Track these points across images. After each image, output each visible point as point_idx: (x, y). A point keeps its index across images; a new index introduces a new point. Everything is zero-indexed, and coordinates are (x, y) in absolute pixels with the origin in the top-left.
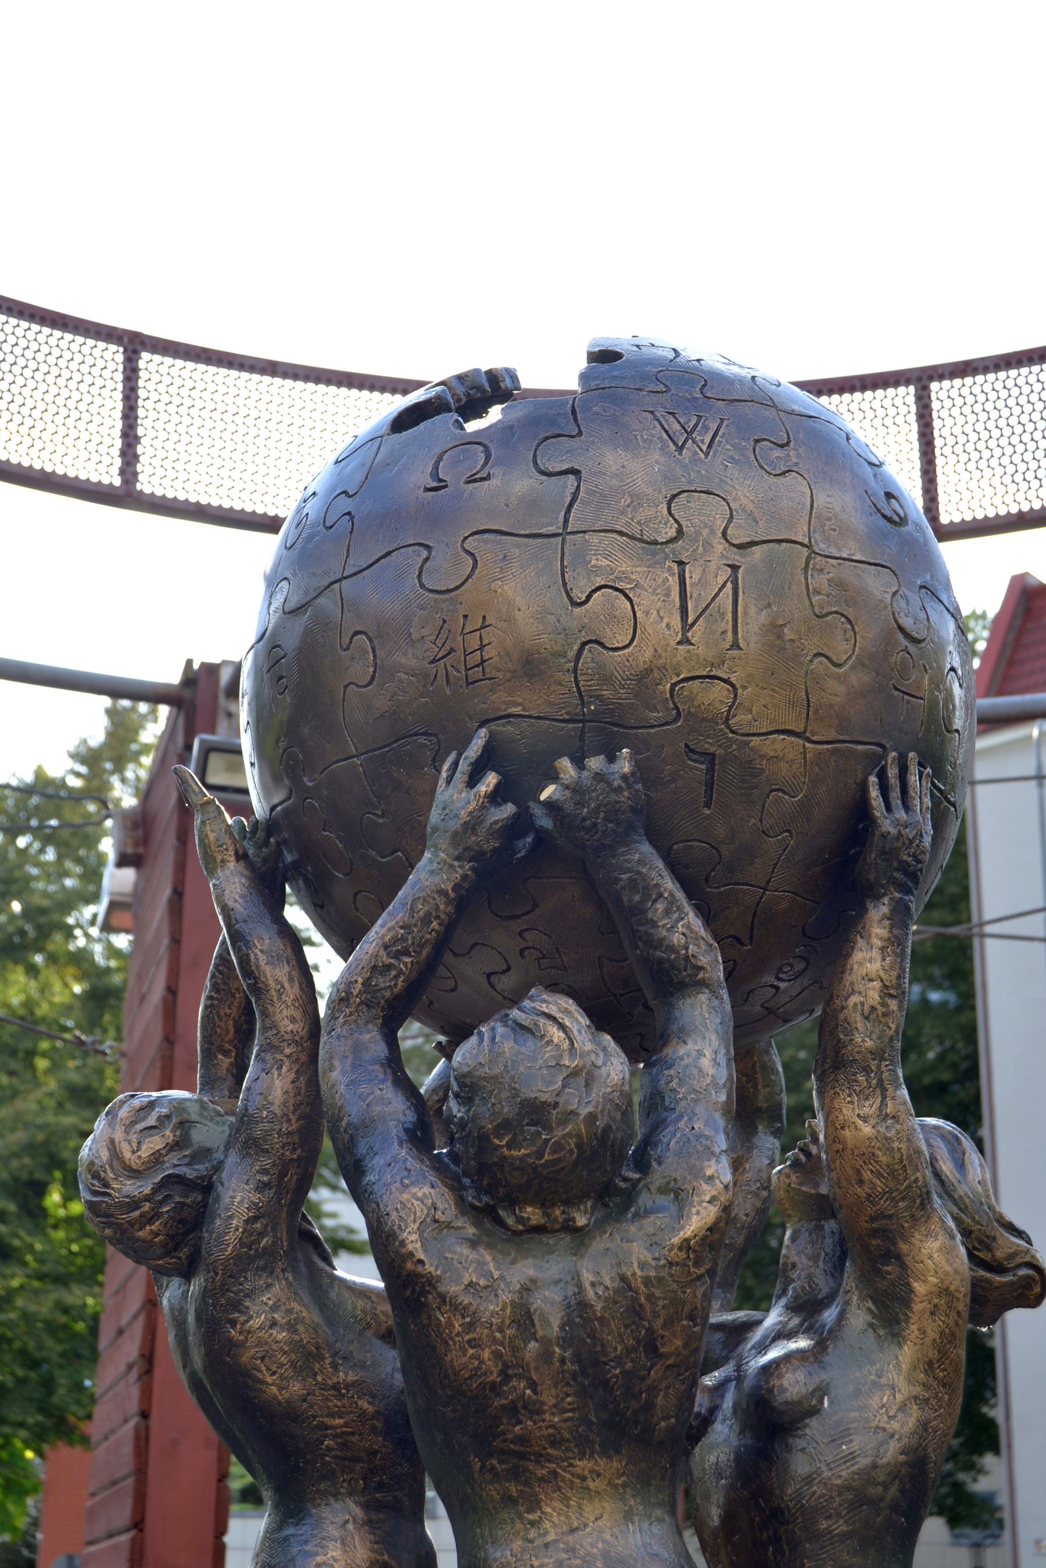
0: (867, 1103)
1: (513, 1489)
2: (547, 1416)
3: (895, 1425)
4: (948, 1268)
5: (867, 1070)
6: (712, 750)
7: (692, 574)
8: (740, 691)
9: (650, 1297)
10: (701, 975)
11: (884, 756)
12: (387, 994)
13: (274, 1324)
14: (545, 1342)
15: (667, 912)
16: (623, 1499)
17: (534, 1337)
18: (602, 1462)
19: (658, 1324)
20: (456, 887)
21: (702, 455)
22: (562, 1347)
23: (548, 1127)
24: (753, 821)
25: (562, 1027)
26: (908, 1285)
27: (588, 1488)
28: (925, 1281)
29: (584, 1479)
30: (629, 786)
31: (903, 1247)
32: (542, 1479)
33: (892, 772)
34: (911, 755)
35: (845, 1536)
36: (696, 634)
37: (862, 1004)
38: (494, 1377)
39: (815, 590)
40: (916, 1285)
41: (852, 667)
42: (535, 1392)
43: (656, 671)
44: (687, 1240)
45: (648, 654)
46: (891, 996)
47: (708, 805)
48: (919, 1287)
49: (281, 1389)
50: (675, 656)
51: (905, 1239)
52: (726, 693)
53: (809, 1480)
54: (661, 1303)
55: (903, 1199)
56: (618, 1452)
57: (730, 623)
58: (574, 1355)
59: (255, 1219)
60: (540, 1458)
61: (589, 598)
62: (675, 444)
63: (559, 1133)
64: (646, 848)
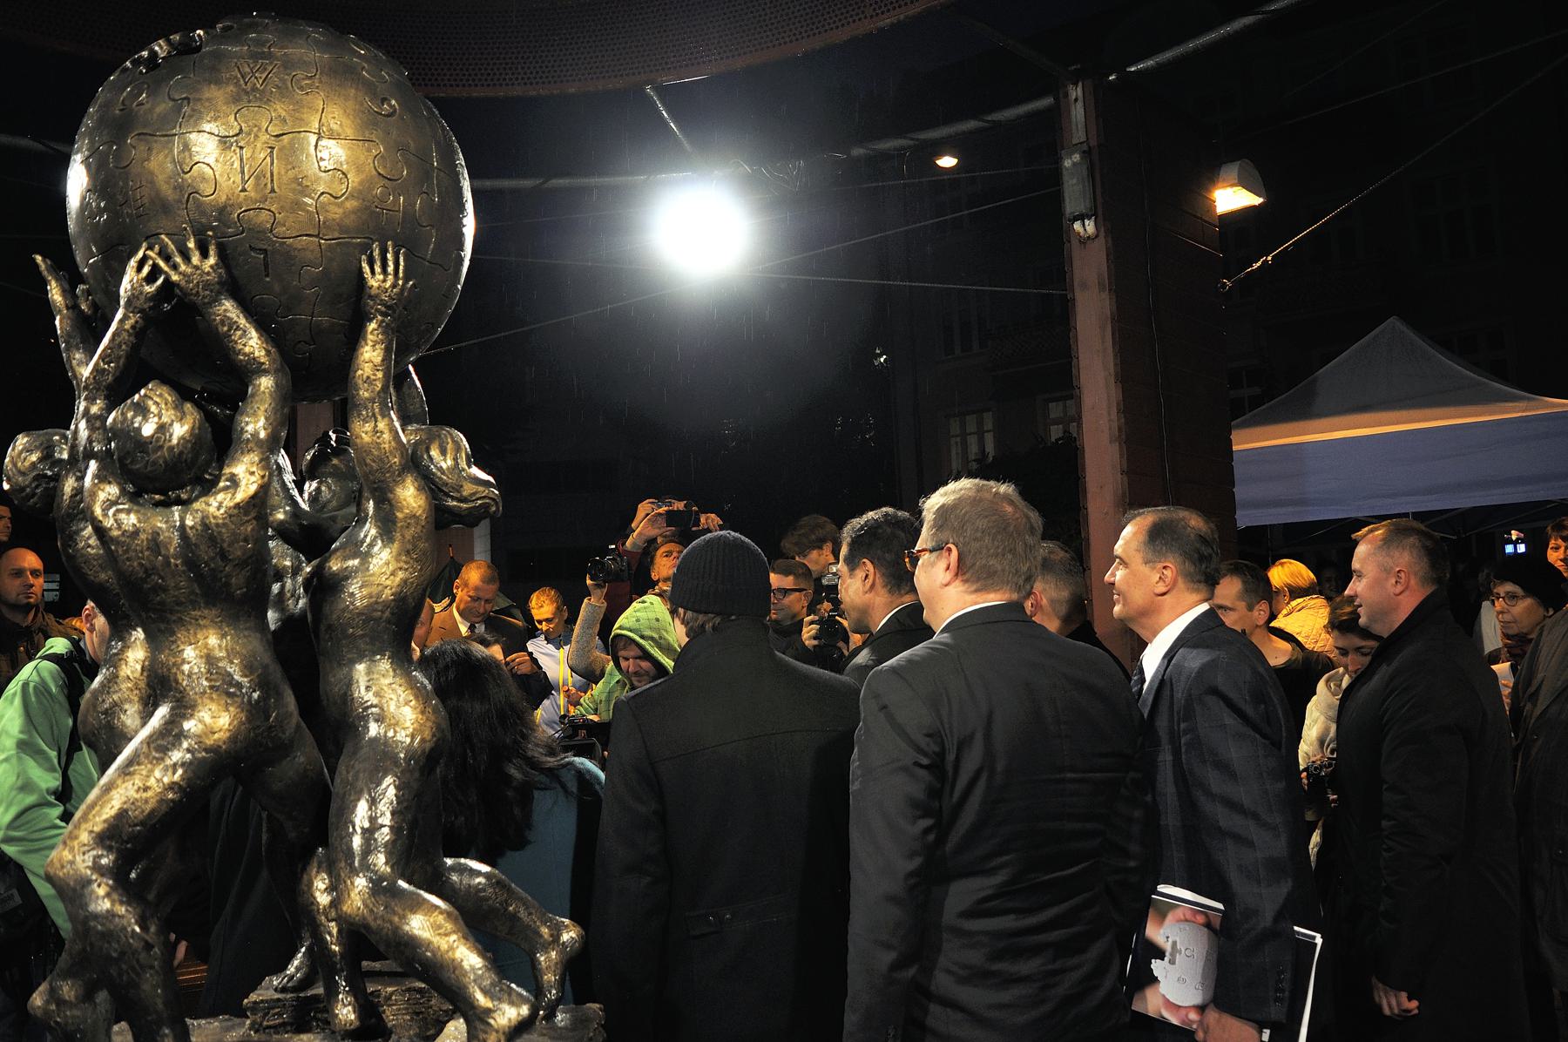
0: (367, 425)
1: (162, 626)
2: (172, 592)
3: (388, 582)
4: (414, 505)
5: (366, 408)
6: (265, 247)
8: (277, 215)
10: (263, 367)
12: (104, 383)
16: (220, 628)
17: (160, 555)
18: (206, 612)
19: (225, 545)
20: (133, 327)
22: (175, 559)
24: (295, 283)
26: (394, 514)
27: (199, 625)
28: (402, 512)
29: (197, 620)
30: (214, 271)
31: (391, 496)
32: (174, 621)
33: (376, 253)
34: (389, 243)
35: (362, 636)
37: (362, 375)
38: (141, 574)
40: (398, 514)
41: (347, 198)
42: (163, 581)
43: (229, 208)
45: (224, 198)
46: (378, 370)
47: (267, 276)
48: (399, 515)
49: (95, 577)
50: (238, 198)
51: (392, 491)
52: (268, 217)
53: (344, 611)
54: (226, 535)
55: (388, 472)
56: (214, 605)
57: (269, 179)
58: (182, 562)
59: (76, 495)
61: (191, 169)
62: (244, 80)
63: (153, 457)
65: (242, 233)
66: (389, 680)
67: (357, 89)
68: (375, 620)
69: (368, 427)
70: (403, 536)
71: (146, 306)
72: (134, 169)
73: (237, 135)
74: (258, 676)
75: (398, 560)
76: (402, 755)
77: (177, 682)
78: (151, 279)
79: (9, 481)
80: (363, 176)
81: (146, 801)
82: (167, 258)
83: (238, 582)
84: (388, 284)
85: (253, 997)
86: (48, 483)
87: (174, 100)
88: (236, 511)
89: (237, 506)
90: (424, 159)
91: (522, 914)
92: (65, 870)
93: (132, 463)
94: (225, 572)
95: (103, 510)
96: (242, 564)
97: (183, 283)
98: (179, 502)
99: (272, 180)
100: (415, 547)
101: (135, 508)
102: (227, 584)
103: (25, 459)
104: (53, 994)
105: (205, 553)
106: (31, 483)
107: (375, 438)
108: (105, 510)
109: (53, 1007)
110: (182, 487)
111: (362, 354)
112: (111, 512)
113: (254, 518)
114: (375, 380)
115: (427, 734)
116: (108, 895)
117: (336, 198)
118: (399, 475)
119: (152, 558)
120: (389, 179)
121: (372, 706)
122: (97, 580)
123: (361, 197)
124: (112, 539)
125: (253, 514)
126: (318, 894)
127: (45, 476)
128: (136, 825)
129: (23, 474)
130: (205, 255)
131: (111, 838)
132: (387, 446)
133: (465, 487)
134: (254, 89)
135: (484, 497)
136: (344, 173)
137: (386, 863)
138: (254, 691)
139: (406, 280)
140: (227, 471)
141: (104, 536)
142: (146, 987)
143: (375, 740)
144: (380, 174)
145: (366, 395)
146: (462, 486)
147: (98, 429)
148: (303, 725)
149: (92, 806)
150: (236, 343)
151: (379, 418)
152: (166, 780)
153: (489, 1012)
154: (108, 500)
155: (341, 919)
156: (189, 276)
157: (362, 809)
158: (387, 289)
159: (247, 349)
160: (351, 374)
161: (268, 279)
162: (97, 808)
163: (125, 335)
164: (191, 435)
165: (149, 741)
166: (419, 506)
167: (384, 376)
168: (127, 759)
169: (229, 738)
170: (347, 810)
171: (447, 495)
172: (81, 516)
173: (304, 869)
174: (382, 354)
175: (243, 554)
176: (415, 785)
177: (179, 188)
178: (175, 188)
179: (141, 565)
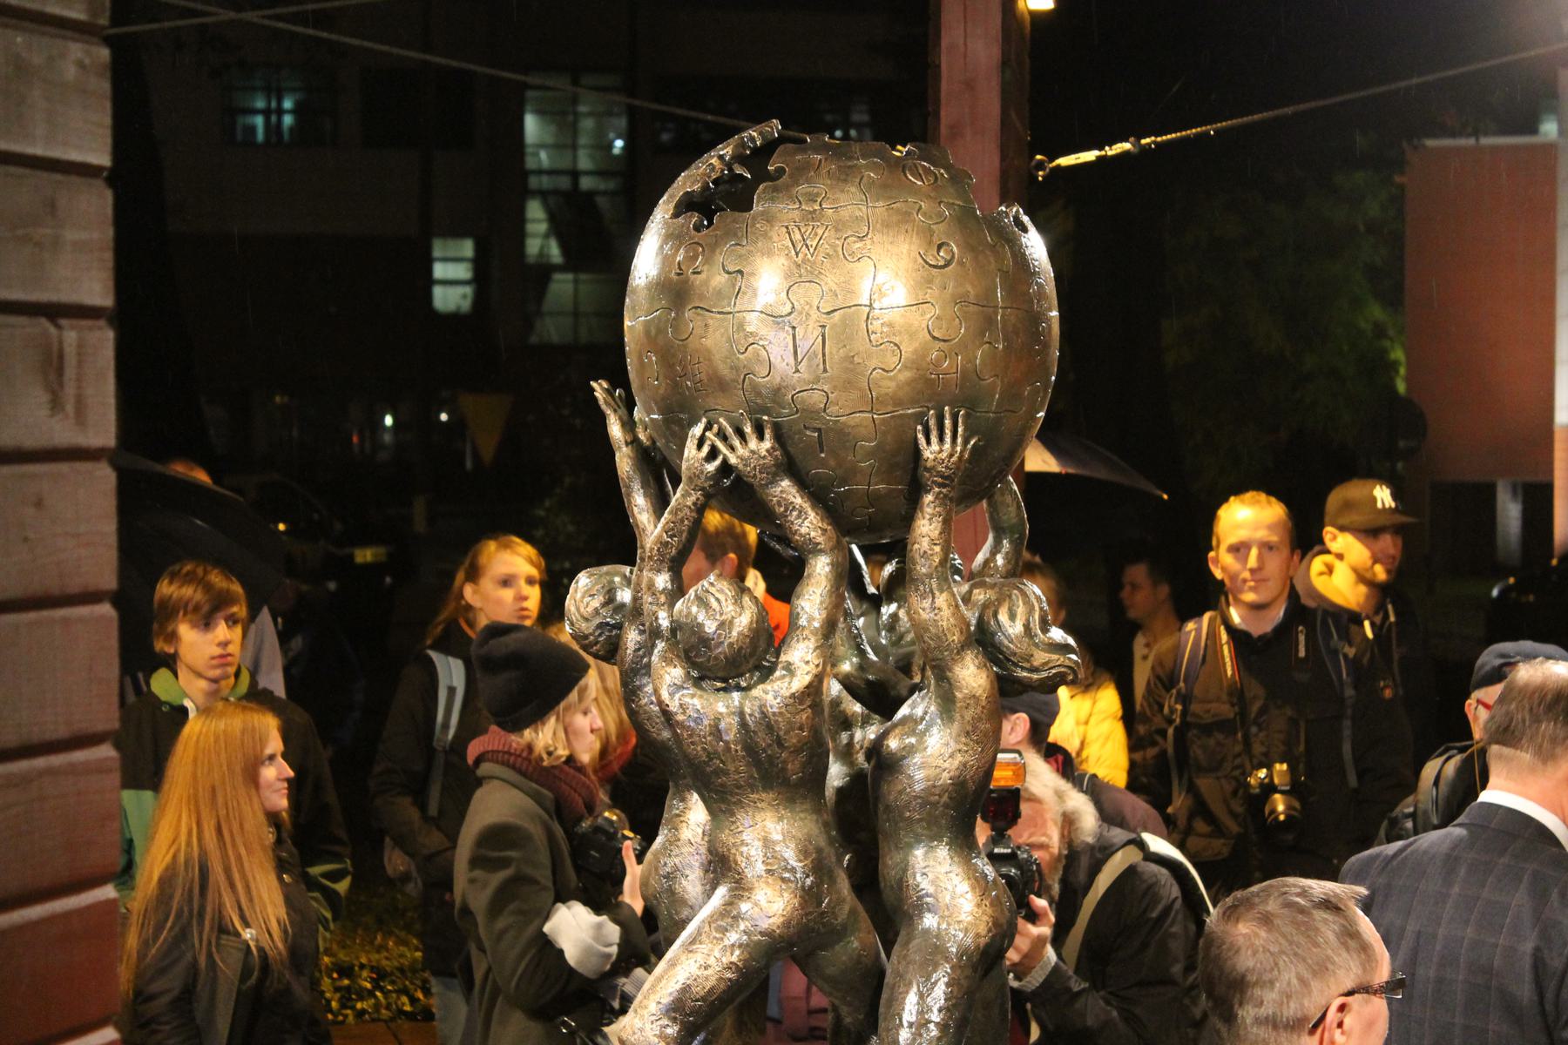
1: (723, 807)
3: (946, 765)
4: (975, 685)
7: (800, 332)
9: (776, 721)
11: (926, 414)
13: (652, 703)
14: (727, 743)
15: (799, 517)
16: (777, 811)
19: (781, 733)
20: (694, 504)
21: (809, 256)
25: (718, 600)
27: (757, 807)
30: (770, 455)
31: (949, 674)
32: (735, 803)
34: (946, 408)
35: (920, 820)
36: (802, 367)
38: (704, 758)
39: (873, 332)
41: (900, 370)
44: (794, 694)
45: (778, 379)
46: (935, 544)
47: (822, 451)
48: (958, 695)
51: (950, 670)
53: (900, 793)
56: (772, 789)
59: (639, 649)
61: (746, 349)
64: (786, 483)
65: (797, 412)
66: (946, 867)
67: (910, 243)
69: (927, 604)
70: (963, 717)
71: (706, 485)
72: (693, 343)
73: (790, 314)
74: (812, 862)
75: (957, 742)
76: (954, 950)
77: (736, 864)
78: (713, 454)
79: (572, 624)
80: (916, 345)
81: (707, 979)
82: (724, 437)
83: (794, 768)
84: (944, 455)
86: (610, 631)
87: (728, 273)
88: (792, 701)
89: (793, 696)
92: (636, 1037)
93: (696, 656)
94: (781, 759)
95: (670, 694)
96: (797, 751)
97: (741, 467)
98: (739, 688)
99: (824, 361)
100: (975, 728)
101: (699, 693)
102: (784, 770)
103: (588, 604)
105: (762, 740)
106: (594, 631)
107: (932, 615)
108: (672, 695)
110: (742, 675)
111: (919, 527)
112: (677, 696)
113: (809, 707)
114: (932, 555)
115: (983, 929)
117: (887, 371)
118: (958, 653)
119: (714, 743)
120: (944, 341)
121: (927, 895)
122: (659, 738)
123: (915, 366)
124: (681, 724)
125: (808, 703)
127: (607, 624)
128: (697, 1000)
129: (587, 620)
131: (674, 1010)
132: (945, 624)
133: (1036, 656)
135: (1059, 666)
136: (896, 345)
138: (808, 876)
139: (966, 442)
140: (783, 658)
141: (671, 720)
143: (927, 931)
144: (934, 338)
145: (924, 570)
146: (1032, 655)
147: (663, 605)
148: (860, 908)
150: (792, 523)
151: (937, 593)
152: (724, 960)
154: (675, 684)
156: (746, 460)
157: (911, 1000)
158: (943, 460)
159: (803, 530)
160: (909, 547)
161: (823, 455)
162: (664, 981)
163: (687, 511)
164: (750, 629)
165: (711, 920)
166: (979, 686)
167: (942, 550)
168: (690, 936)
169: (783, 923)
170: (897, 1003)
171: (1016, 665)
172: (644, 671)
174: (939, 528)
175: (799, 742)
176: (964, 983)
177: (735, 368)
178: (731, 368)
179: (704, 749)
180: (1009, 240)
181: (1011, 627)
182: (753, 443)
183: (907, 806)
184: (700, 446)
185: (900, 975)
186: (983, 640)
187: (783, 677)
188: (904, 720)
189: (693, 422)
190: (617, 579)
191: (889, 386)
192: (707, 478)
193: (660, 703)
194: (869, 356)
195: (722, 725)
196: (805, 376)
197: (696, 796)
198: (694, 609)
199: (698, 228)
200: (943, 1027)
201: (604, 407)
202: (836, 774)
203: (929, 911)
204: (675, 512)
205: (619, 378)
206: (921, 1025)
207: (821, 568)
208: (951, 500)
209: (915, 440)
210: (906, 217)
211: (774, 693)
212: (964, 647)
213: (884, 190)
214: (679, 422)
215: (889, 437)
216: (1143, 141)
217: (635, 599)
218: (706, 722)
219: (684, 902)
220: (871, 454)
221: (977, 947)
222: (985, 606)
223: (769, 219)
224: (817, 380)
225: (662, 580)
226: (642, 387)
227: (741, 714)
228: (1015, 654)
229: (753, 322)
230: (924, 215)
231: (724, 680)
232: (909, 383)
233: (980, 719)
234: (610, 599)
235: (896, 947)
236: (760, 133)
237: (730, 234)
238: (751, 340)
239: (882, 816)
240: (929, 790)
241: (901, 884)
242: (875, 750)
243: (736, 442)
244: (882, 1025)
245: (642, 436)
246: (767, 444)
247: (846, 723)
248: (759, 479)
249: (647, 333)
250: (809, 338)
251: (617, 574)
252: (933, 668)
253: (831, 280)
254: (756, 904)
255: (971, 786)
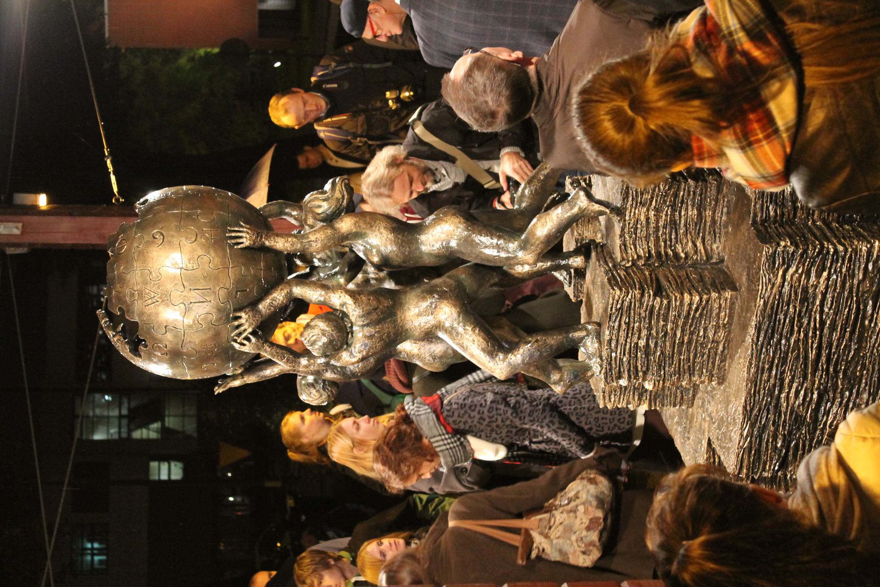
1: (404, 334)
3: (385, 236)
14: (375, 332)
15: (275, 301)
23: (334, 340)
31: (345, 234)
35: (409, 247)
48: (354, 231)
53: (397, 256)
56: (396, 313)
60: (398, 330)
64: (261, 306)
66: (430, 235)
67: (153, 251)
68: (402, 243)
69: (314, 244)
72: (198, 348)
75: (375, 231)
76: (466, 233)
78: (247, 339)
79: (323, 402)
80: (198, 248)
81: (479, 341)
82: (240, 334)
83: (387, 303)
84: (248, 236)
85: (572, 297)
90: (180, 218)
91: (546, 172)
96: (379, 301)
98: (351, 327)
100: (369, 223)
102: (387, 307)
104: (555, 383)
105: (374, 316)
108: (354, 357)
109: (562, 383)
110: (346, 326)
112: (355, 354)
115: (457, 220)
116: (515, 356)
121: (442, 244)
126: (524, 271)
129: (321, 395)
130: (240, 317)
131: (492, 355)
134: (161, 298)
137: (513, 243)
139: (242, 226)
140: (338, 308)
142: (552, 342)
143: (458, 245)
145: (299, 245)
148: (447, 274)
149: (479, 361)
152: (471, 333)
153: (580, 208)
155: (535, 263)
159: (281, 299)
165: (453, 339)
170: (488, 258)
171: (341, 205)
173: (512, 275)
176: (480, 228)
177: (209, 329)
180: (151, 208)
181: (324, 207)
182: (243, 321)
183: (403, 254)
184: (244, 345)
185: (477, 256)
186: (330, 219)
187: (346, 307)
188: (365, 254)
189: (233, 348)
190: (303, 382)
191: (217, 261)
192: (258, 341)
193: (358, 362)
194: (204, 269)
195: (368, 334)
196: (212, 297)
197: (399, 347)
198: (317, 347)
199: (146, 346)
200: (499, 238)
201: (226, 388)
202: (389, 285)
203: (449, 243)
204: (273, 356)
205: (213, 382)
206: (498, 247)
207: (298, 291)
208: (268, 233)
209: (241, 249)
210: (141, 253)
211: (354, 312)
212: (333, 228)
213: (129, 263)
214: (233, 354)
215: (241, 260)
216: (107, 154)
217: (312, 374)
218: (366, 342)
219: (445, 352)
220: (248, 269)
221: (465, 223)
222: (315, 219)
223: (141, 314)
224: (214, 292)
225: (304, 361)
226: (218, 371)
227: (363, 326)
228: (336, 206)
229: (188, 321)
230: (140, 245)
231: (348, 333)
232: (216, 252)
233: (365, 221)
234: (312, 385)
235: (465, 258)
236: (103, 319)
237: (148, 331)
238: (196, 322)
239: (408, 264)
240: (397, 244)
241: (438, 256)
242: (379, 267)
243: (242, 328)
244: (499, 264)
245: (240, 371)
246: (243, 315)
247: (367, 281)
248: (259, 319)
249: (193, 369)
250: (195, 296)
251: (301, 382)
252: (342, 241)
253: (169, 286)
254: (446, 319)
255: (394, 225)
